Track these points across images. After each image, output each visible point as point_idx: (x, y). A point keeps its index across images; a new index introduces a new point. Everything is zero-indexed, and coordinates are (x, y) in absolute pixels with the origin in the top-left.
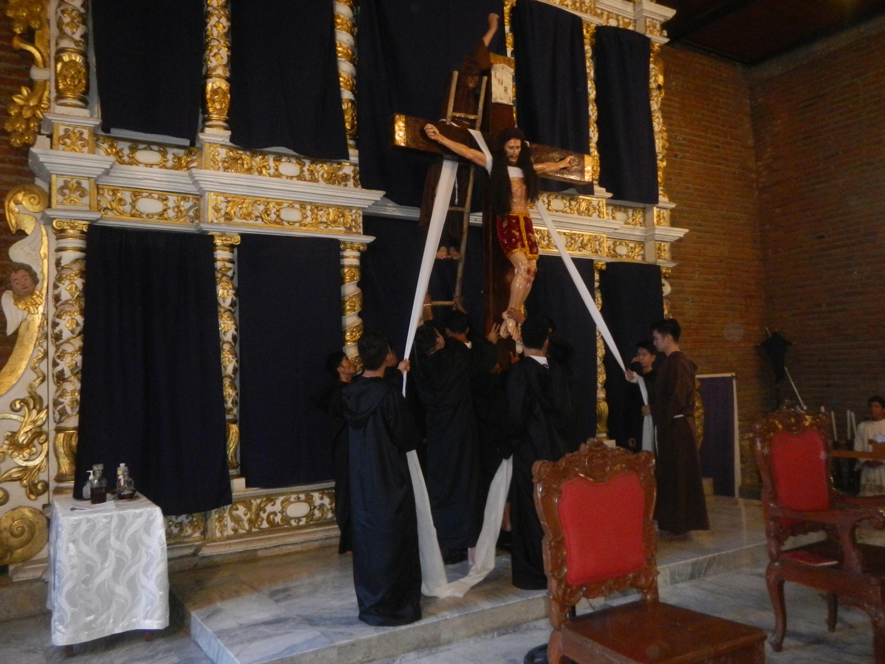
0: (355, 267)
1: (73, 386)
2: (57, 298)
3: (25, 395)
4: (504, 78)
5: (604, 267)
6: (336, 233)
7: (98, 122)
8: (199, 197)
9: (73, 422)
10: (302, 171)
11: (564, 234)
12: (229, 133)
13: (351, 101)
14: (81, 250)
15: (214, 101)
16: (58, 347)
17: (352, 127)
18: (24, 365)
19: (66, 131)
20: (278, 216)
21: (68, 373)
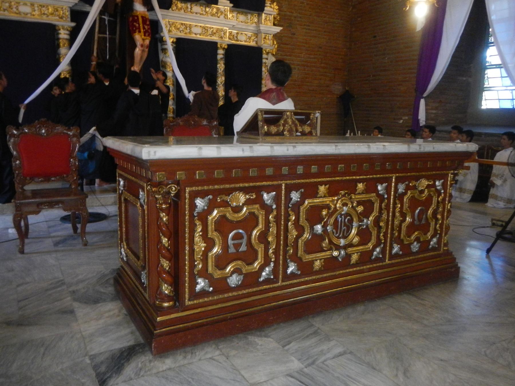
0: (67, 39)
5: (226, 47)
6: (53, 20)
11: (201, 26)
20: (17, 9)
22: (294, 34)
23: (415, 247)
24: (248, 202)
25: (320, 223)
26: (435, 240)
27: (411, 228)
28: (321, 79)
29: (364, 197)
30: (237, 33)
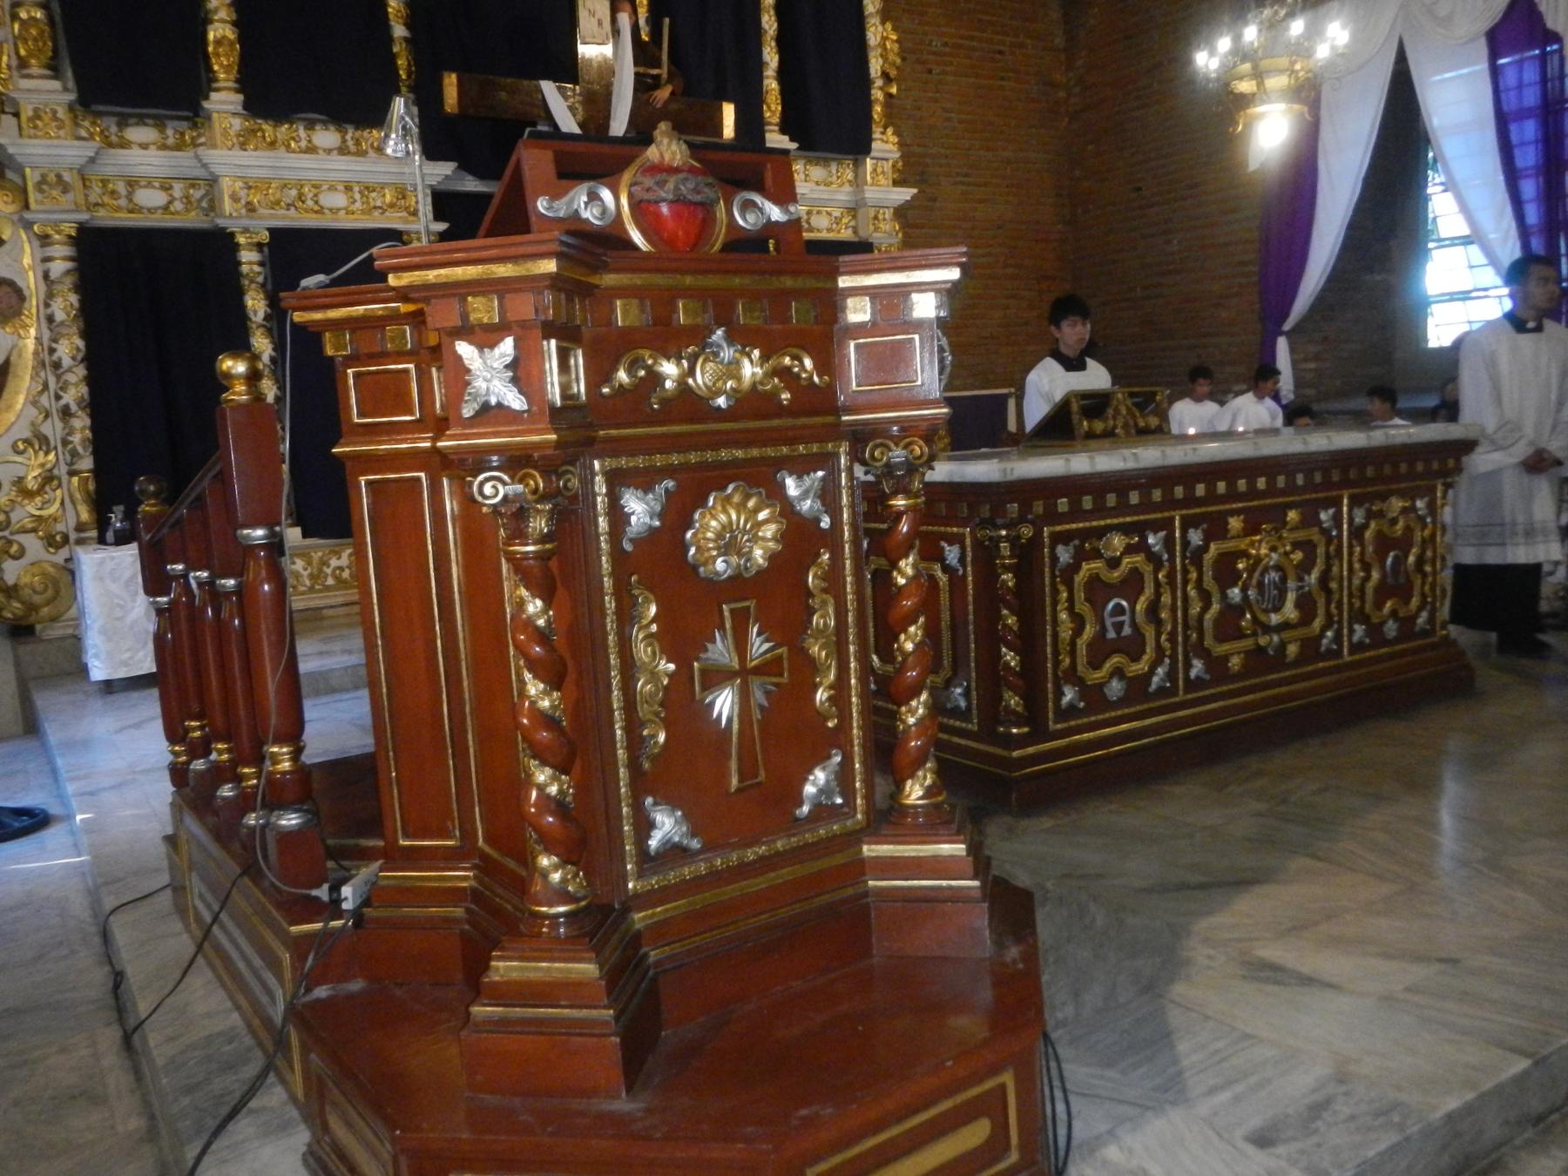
1: (81, 422)
2: (50, 319)
3: (27, 434)
4: (598, 7)
7: (72, 97)
8: (213, 181)
9: (87, 463)
10: (344, 141)
12: (240, 97)
13: (406, 39)
14: (71, 259)
15: (218, 55)
16: (58, 377)
17: (409, 76)
18: (21, 399)
19: (36, 110)
21: (74, 408)
22: (935, 200)
23: (1391, 628)
24: (1129, 550)
25: (1234, 584)
26: (1424, 614)
27: (1383, 592)
28: (1008, 308)
29: (1301, 535)
30: (809, 213)
